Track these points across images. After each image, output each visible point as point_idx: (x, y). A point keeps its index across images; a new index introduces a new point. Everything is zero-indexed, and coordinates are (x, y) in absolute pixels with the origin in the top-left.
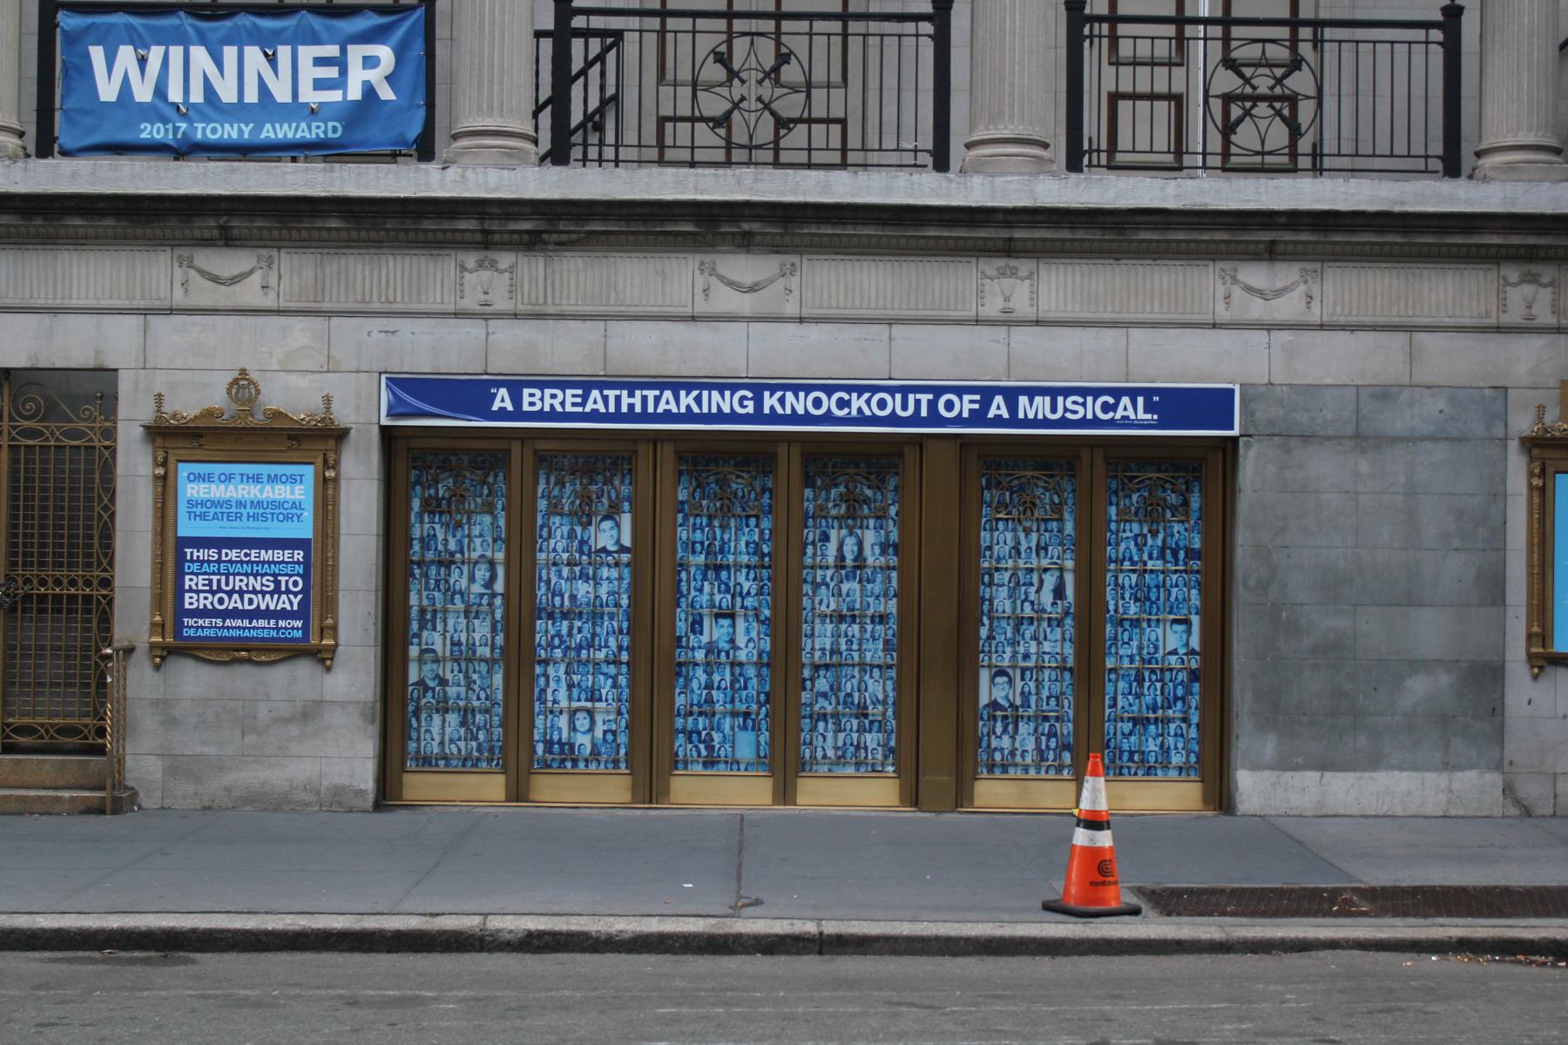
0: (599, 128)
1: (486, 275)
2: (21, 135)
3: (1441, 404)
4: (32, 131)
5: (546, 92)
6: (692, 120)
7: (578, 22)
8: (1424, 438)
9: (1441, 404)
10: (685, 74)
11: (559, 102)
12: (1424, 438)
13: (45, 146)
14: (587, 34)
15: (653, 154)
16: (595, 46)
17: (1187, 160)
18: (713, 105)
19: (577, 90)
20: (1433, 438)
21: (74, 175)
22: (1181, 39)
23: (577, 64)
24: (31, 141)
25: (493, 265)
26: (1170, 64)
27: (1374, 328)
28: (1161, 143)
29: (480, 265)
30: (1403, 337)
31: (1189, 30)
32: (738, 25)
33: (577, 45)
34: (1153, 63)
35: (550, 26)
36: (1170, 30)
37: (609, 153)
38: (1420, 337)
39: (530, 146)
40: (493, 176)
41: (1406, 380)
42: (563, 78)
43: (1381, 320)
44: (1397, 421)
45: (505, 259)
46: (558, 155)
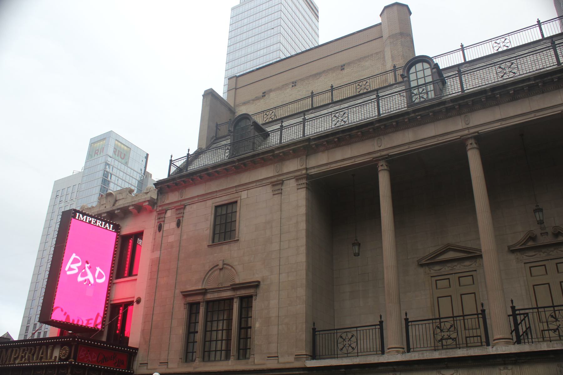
0: (527, 334)
1: (506, 371)
2: (403, 348)
4: (405, 347)
5: (513, 328)
6: (548, 330)
7: (517, 312)
10: (544, 320)
11: (516, 330)
13: (409, 351)
14: (520, 314)
15: (541, 340)
16: (522, 317)
18: (552, 327)
19: (520, 327)
21: (415, 356)
23: (519, 321)
24: (406, 350)
25: (507, 369)
29: (504, 369)
32: (556, 308)
33: (518, 317)
35: (511, 314)
37: (530, 340)
39: (511, 341)
40: (504, 348)
42: (516, 324)
45: (510, 367)
46: (519, 342)
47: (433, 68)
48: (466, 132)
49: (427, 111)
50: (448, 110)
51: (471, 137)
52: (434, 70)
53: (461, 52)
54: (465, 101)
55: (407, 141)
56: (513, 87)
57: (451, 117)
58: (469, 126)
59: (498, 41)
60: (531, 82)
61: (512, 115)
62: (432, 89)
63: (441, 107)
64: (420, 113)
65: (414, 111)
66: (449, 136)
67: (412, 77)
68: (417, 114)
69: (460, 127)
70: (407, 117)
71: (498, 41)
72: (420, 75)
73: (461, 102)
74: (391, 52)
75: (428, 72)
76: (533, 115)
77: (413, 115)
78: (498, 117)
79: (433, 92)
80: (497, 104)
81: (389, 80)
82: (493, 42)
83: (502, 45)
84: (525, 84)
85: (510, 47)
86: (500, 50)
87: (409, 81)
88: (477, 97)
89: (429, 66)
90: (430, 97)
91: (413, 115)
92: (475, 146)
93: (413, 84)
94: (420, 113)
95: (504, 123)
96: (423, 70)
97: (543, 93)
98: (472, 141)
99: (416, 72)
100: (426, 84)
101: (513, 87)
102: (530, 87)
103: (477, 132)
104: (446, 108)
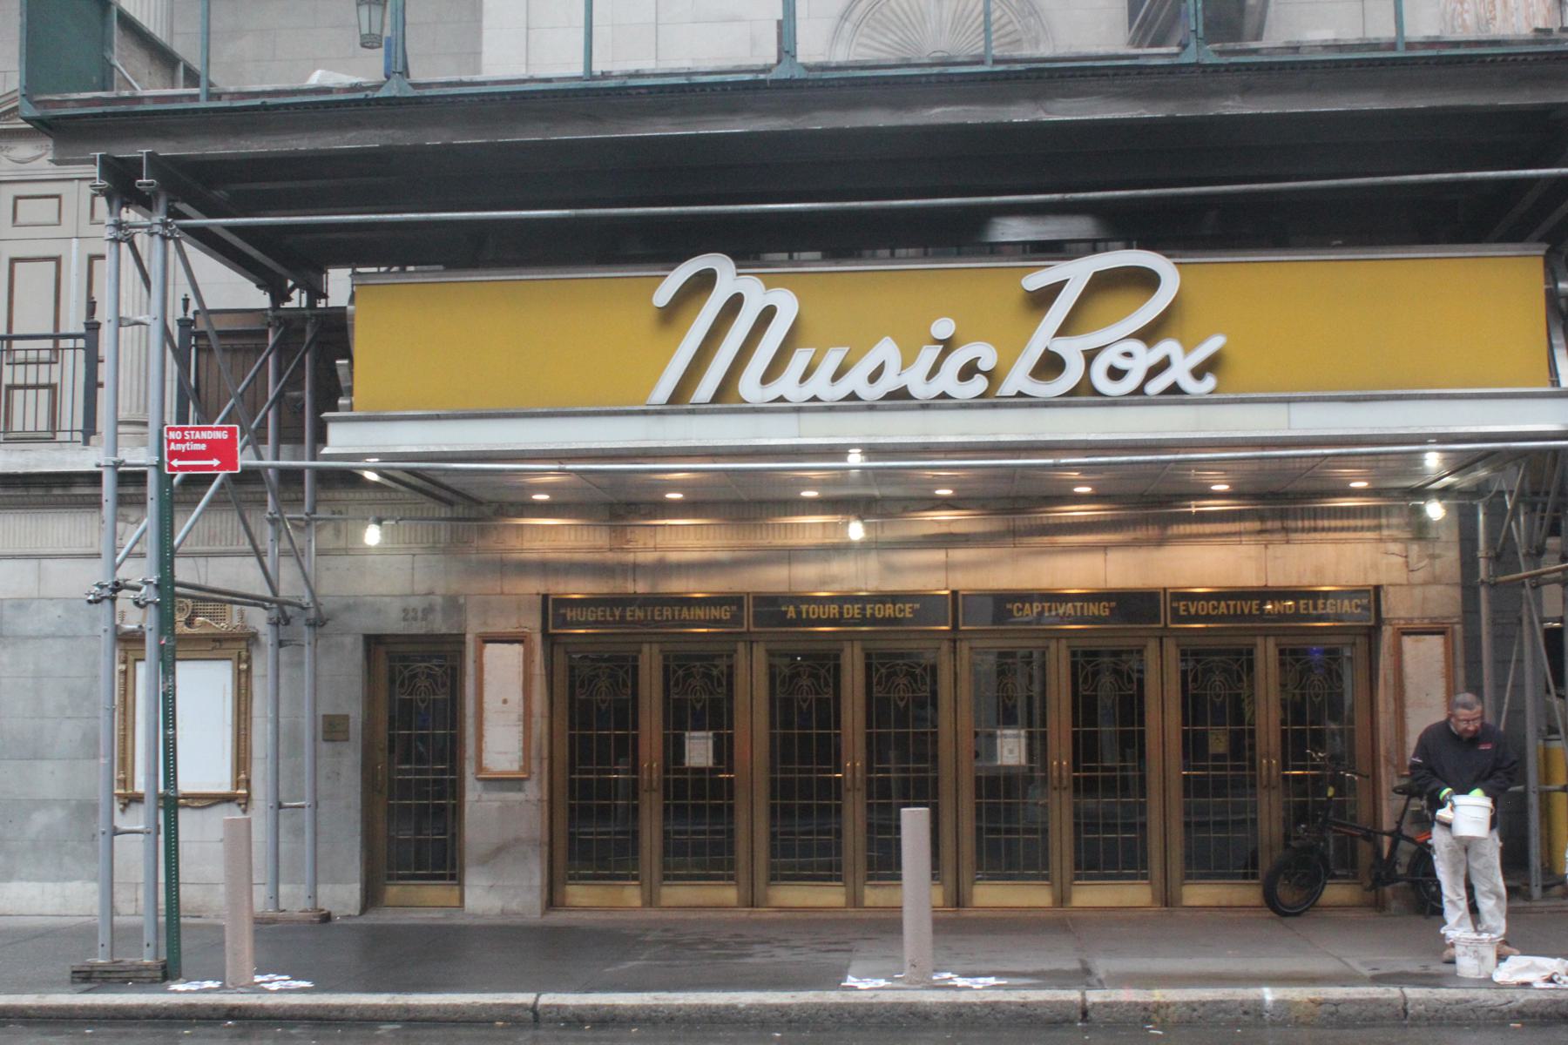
3: (59, 612)
8: (46, 637)
9: (59, 612)
12: (46, 637)
17: (60, 437)
20: (53, 636)
22: (56, 349)
26: (50, 363)
27: (13, 557)
28: (43, 425)
30: (34, 562)
31: (63, 343)
34: (38, 363)
36: (49, 343)
38: (45, 562)
41: (35, 595)
43: (18, 551)
44: (28, 624)
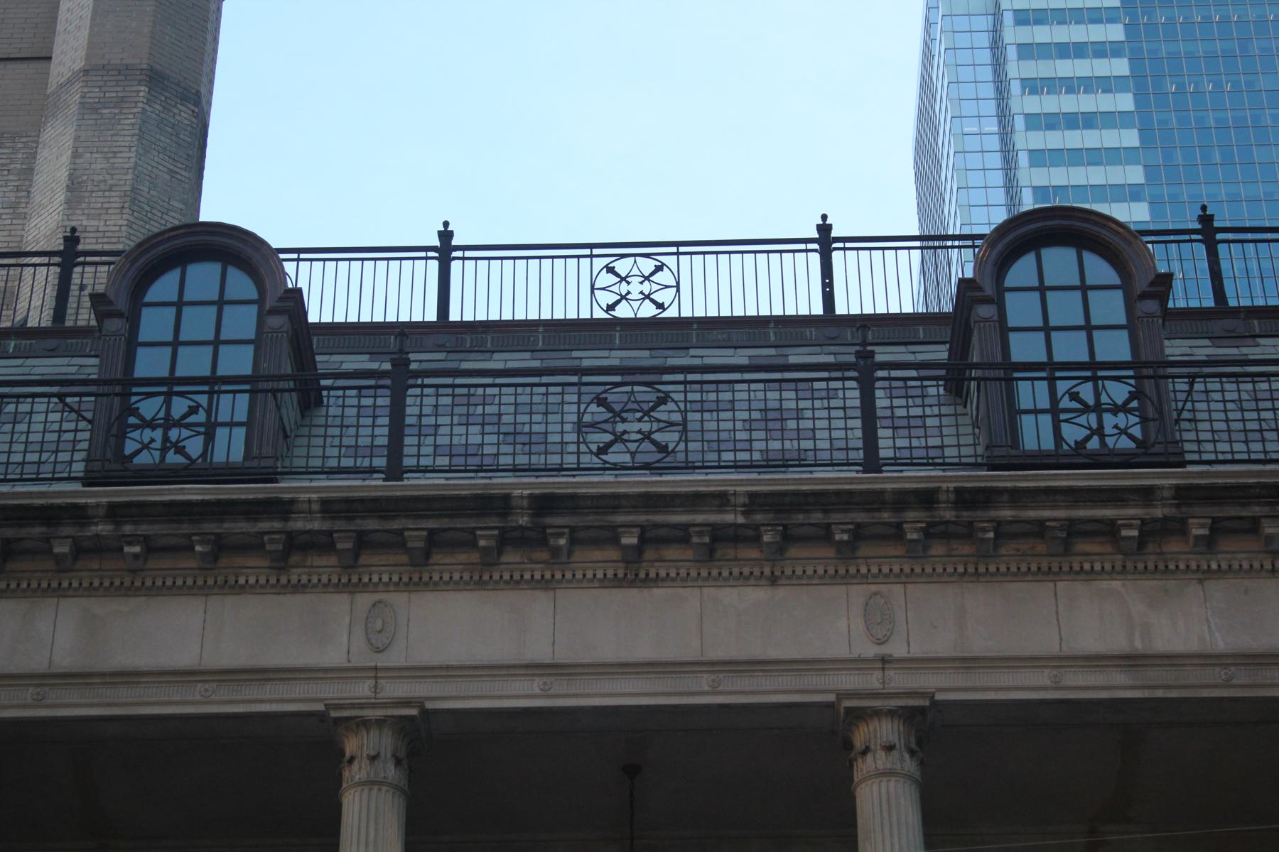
47: (274, 312)
48: (363, 690)
49: (185, 528)
50: (298, 545)
51: (380, 723)
52: (275, 322)
53: (434, 266)
54: (395, 525)
55: (36, 662)
56: (642, 518)
57: (299, 588)
58: (382, 661)
59: (623, 267)
60: (729, 518)
61: (608, 653)
62: (241, 415)
63: (264, 525)
64: (144, 529)
65: (115, 513)
66: (269, 691)
67: (155, 324)
68: (128, 529)
69: (333, 656)
70: (68, 530)
71: (623, 267)
72: (198, 324)
73: (371, 524)
74: (76, 155)
75: (242, 322)
76: (705, 682)
77: (103, 529)
78: (539, 650)
79: (240, 433)
80: (545, 584)
81: (22, 305)
82: (600, 263)
83: (635, 288)
84: (700, 518)
85: (671, 313)
86: (623, 311)
87: (132, 344)
88: (460, 523)
89: (253, 294)
90: (219, 456)
91: (103, 529)
92: (391, 772)
93: (150, 364)
94: (144, 529)
95: (560, 686)
96: (221, 303)
97: (773, 581)
98: (383, 742)
99: (180, 304)
100: (214, 383)
101: (642, 518)
102: (721, 537)
103: (419, 703)
104: (290, 535)
